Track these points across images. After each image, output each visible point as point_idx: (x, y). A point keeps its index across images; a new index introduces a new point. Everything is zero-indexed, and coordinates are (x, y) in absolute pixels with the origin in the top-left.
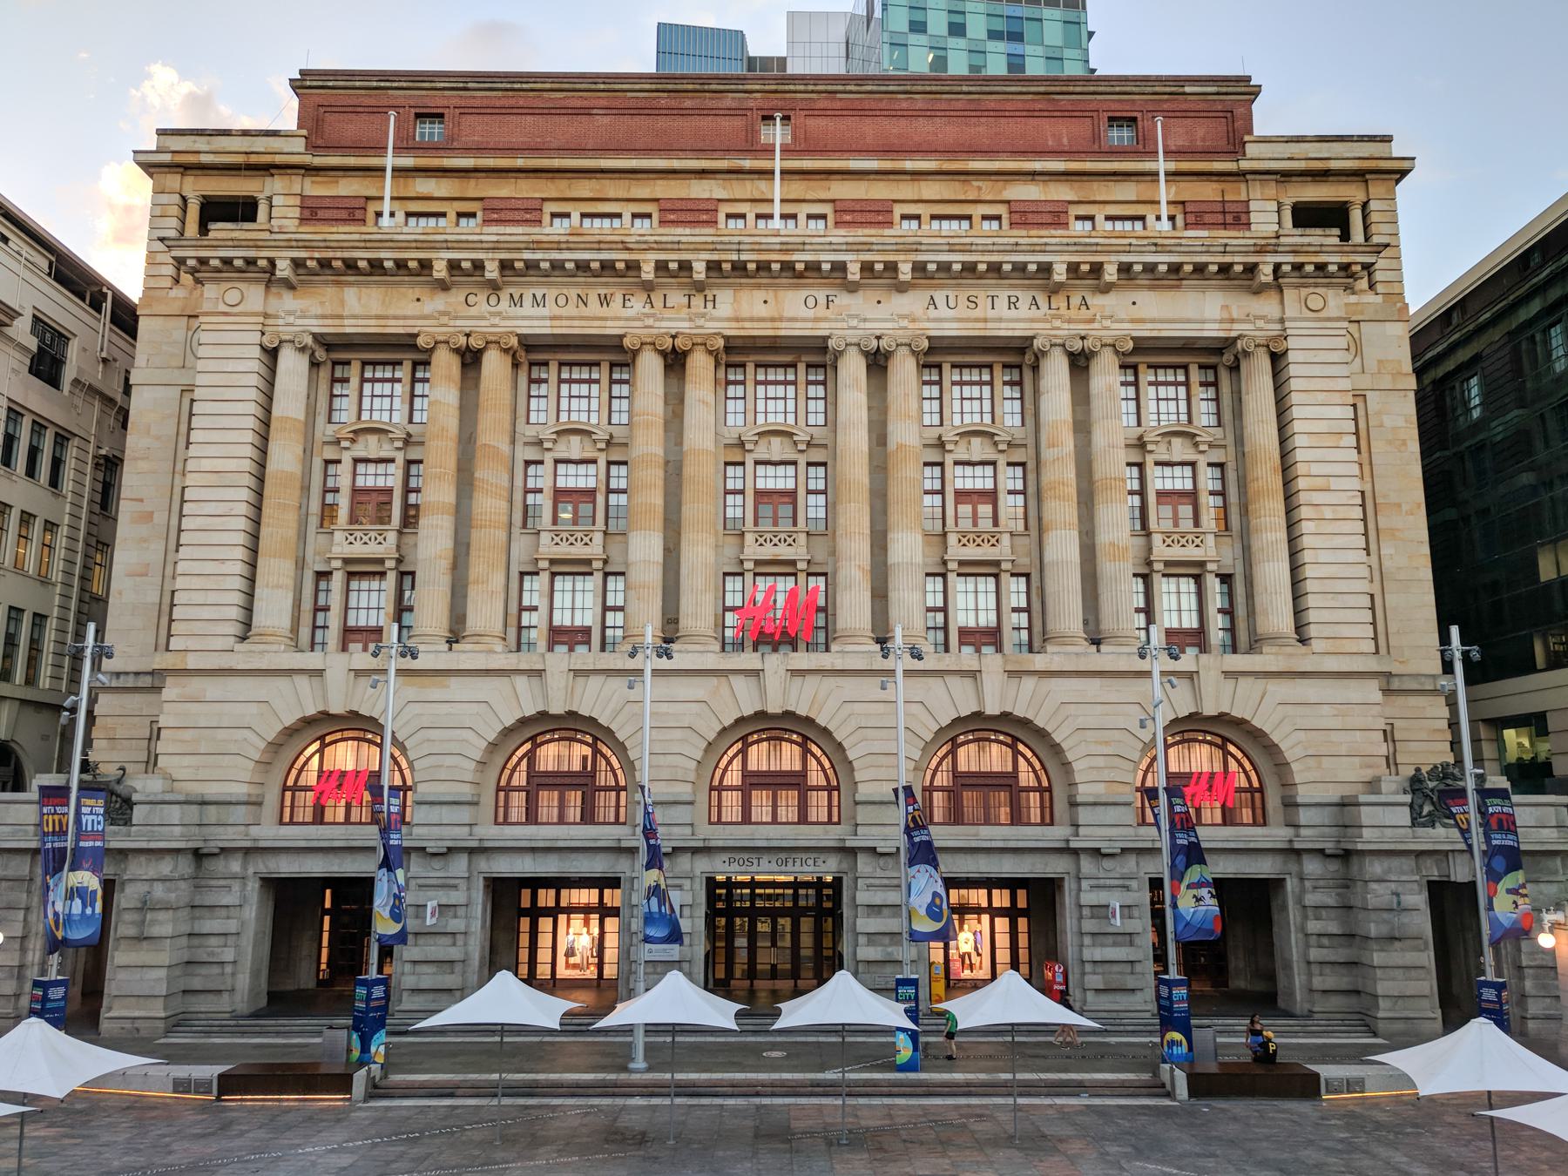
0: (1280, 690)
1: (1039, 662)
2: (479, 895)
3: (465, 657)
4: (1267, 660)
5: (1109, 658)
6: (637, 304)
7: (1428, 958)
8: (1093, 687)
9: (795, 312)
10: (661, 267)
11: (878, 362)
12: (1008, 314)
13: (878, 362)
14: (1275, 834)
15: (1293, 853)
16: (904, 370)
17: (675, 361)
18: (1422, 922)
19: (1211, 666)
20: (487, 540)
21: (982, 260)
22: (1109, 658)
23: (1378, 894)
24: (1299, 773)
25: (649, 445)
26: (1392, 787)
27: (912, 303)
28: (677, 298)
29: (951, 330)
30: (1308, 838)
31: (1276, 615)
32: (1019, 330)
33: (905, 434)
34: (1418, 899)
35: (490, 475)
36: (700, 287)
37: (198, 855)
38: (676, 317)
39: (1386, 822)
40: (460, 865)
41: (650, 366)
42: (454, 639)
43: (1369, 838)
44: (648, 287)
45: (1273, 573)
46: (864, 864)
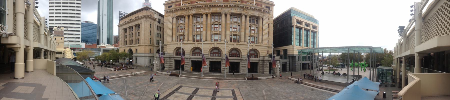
0: (260, 47)
1: (239, 43)
2: (190, 62)
3: (189, 42)
4: (259, 44)
5: (246, 43)
6: (203, 10)
7: (268, 68)
8: (244, 46)
9: (218, 10)
10: (205, 6)
11: (226, 15)
12: (239, 11)
13: (226, 15)
14: (258, 59)
15: (259, 60)
16: (228, 16)
17: (207, 15)
18: (268, 66)
19: (254, 45)
20: (190, 32)
21: (237, 5)
22: (246, 43)
23: (265, 64)
24: (261, 54)
25: (204, 23)
26: (267, 55)
27: (229, 9)
28: (207, 9)
29: (233, 12)
30: (261, 59)
31: (260, 41)
32: (240, 13)
33: (228, 22)
34: (268, 64)
35: (191, 27)
36: (209, 8)
37: (170, 58)
38: (207, 11)
39: (267, 58)
40: (189, 59)
41: (204, 16)
42: (188, 41)
43: (265, 59)
44: (204, 8)
45: (260, 37)
46: (223, 60)
